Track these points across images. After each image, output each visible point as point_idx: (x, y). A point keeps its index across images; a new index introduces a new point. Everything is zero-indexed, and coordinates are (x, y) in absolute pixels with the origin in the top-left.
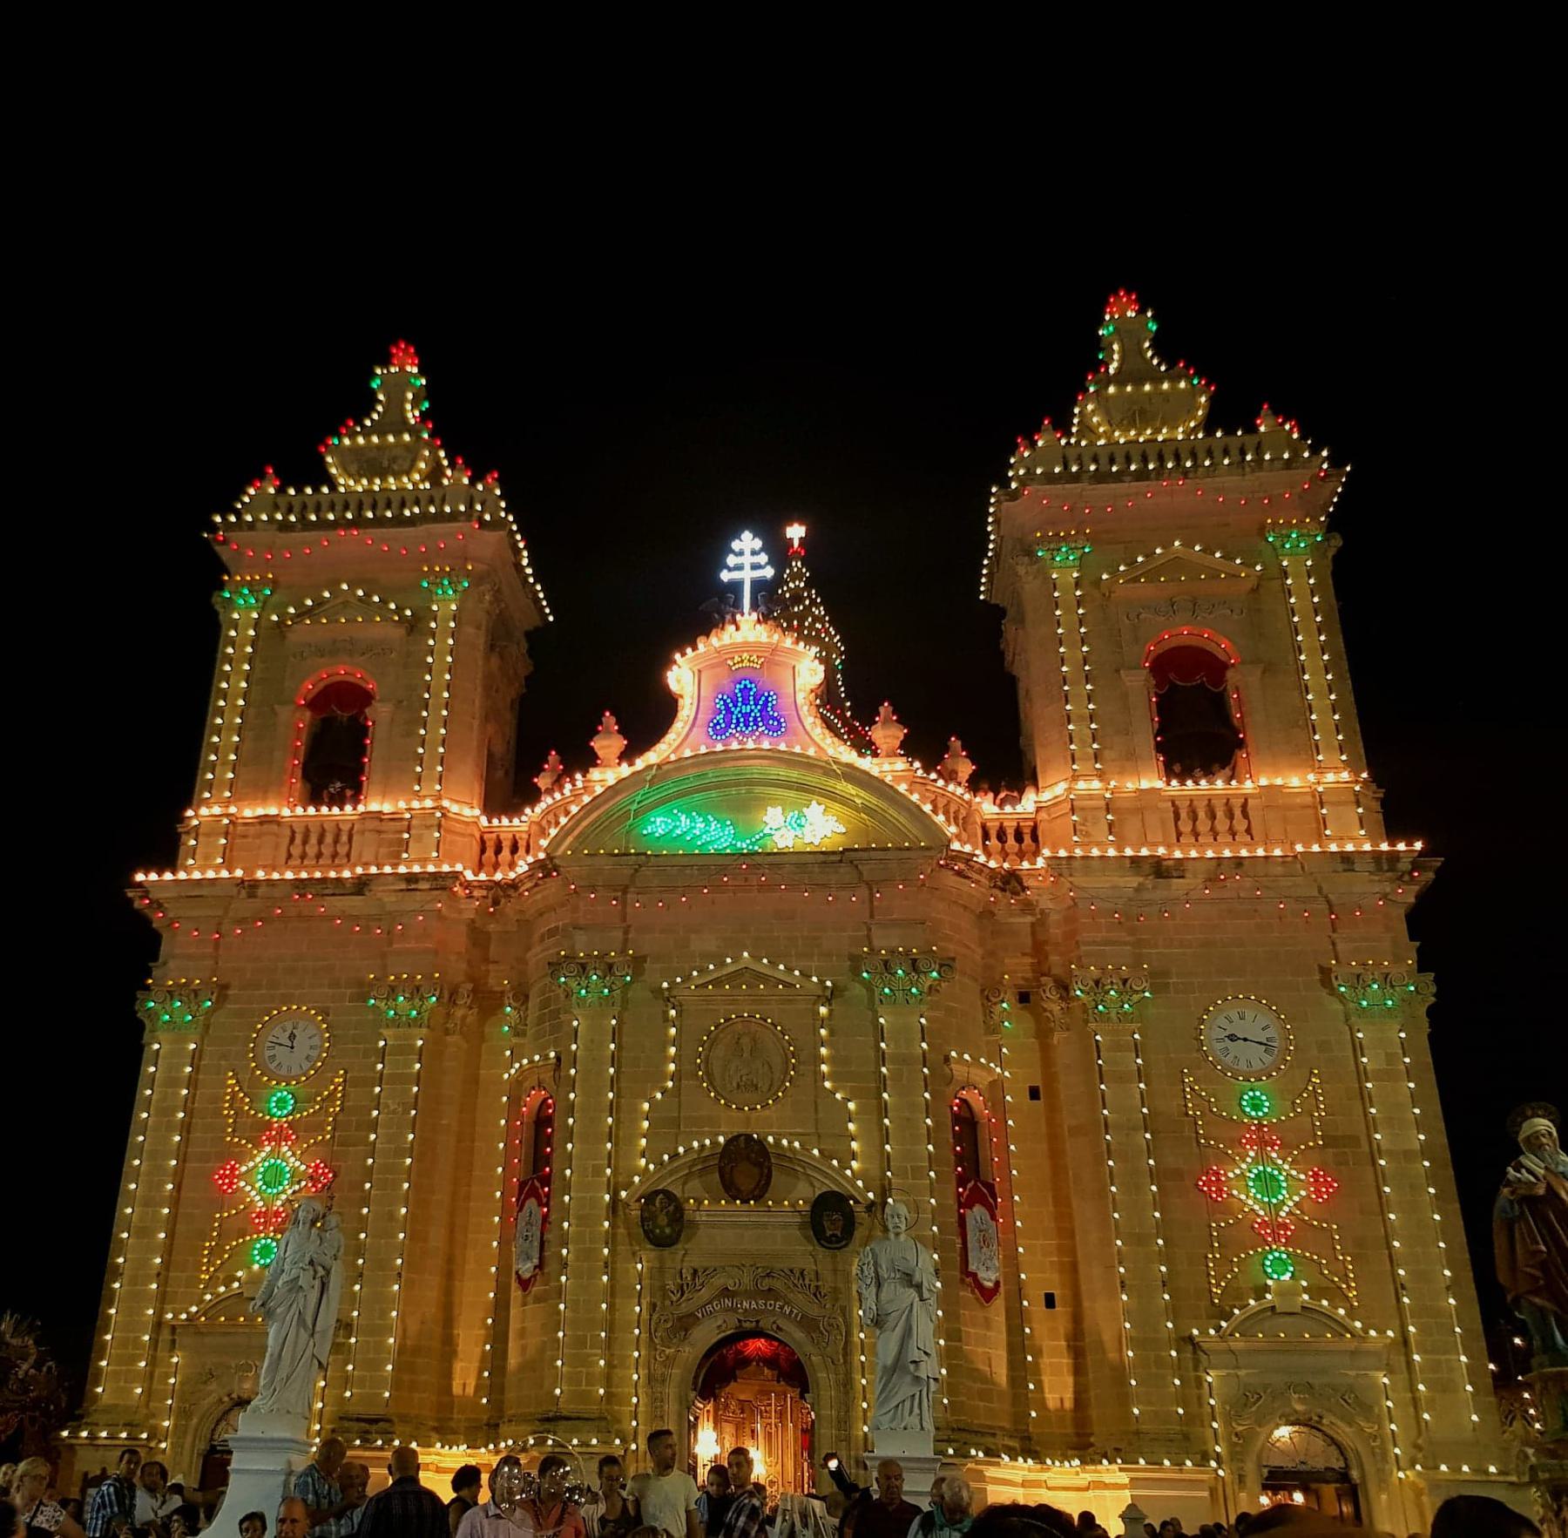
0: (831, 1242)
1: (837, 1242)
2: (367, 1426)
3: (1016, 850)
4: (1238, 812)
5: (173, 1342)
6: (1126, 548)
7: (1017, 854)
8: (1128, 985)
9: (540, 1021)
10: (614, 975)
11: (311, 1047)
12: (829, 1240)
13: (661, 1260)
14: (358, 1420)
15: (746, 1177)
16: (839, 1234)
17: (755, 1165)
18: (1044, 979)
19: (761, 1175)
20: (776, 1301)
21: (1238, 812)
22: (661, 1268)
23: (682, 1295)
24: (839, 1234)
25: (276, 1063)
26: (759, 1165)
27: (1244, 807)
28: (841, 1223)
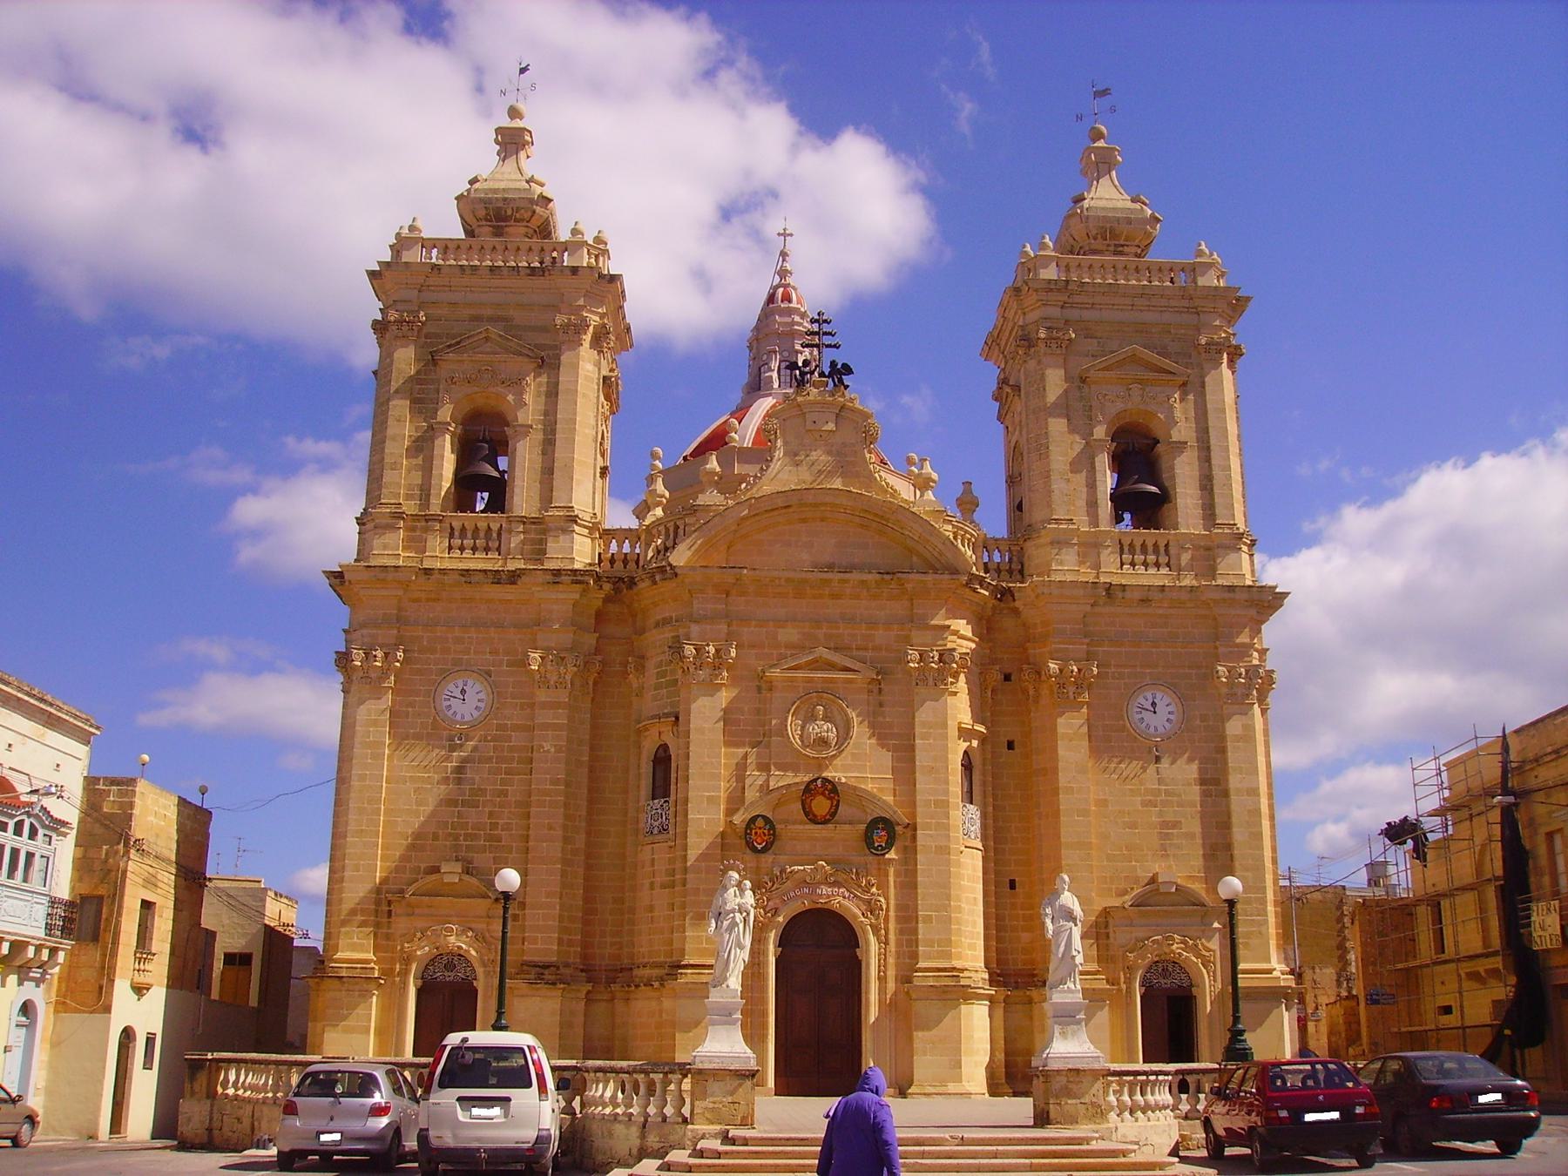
0: (878, 850)
1: (881, 850)
2: (542, 971)
3: (1007, 568)
4: (1162, 550)
5: (390, 911)
6: (1099, 342)
7: (1007, 571)
8: (1082, 673)
9: (658, 687)
10: (721, 657)
11: (479, 701)
12: (876, 849)
13: (758, 861)
14: (535, 966)
15: (821, 805)
16: (884, 845)
17: (828, 799)
18: (1025, 667)
19: (832, 806)
20: (839, 889)
21: (1162, 550)
22: (758, 867)
23: (773, 885)
24: (884, 845)
25: (452, 712)
26: (831, 799)
27: (1167, 546)
28: (886, 838)
